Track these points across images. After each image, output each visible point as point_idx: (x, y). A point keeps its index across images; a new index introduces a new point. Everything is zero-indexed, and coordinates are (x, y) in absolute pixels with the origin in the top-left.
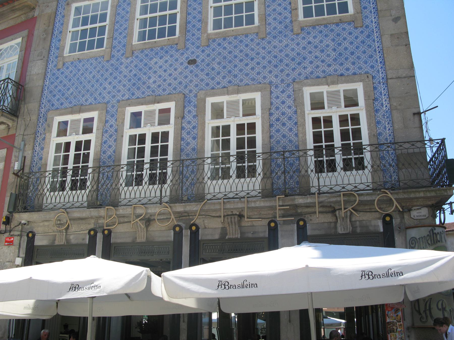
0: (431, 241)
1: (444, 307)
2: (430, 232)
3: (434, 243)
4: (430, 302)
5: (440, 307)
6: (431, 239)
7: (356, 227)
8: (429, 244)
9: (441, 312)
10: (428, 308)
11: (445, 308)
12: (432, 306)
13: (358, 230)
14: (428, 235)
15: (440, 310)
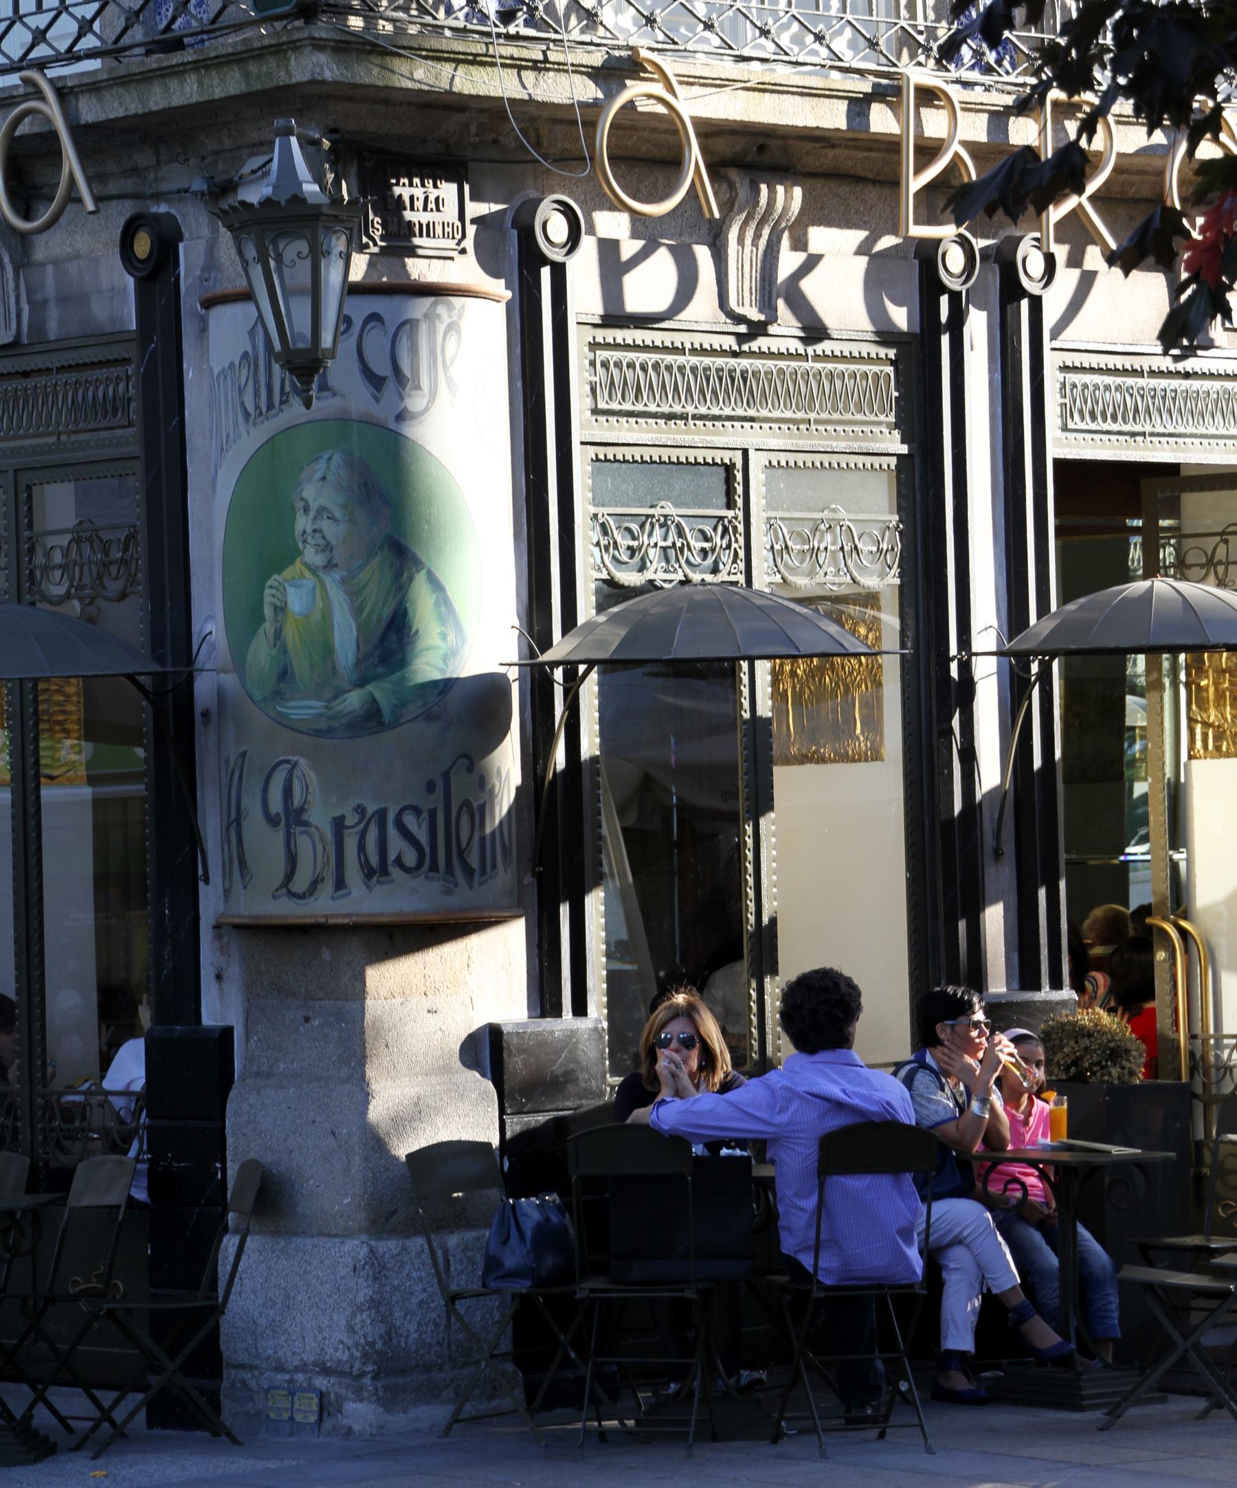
0: (257, 394)
1: (297, 800)
2: (252, 333)
3: (270, 406)
4: (240, 778)
5: (276, 806)
6: (256, 381)
7: (45, 302)
8: (247, 415)
9: (279, 836)
10: (233, 815)
11: (302, 810)
12: (245, 802)
13: (53, 329)
14: (245, 355)
15: (273, 821)
